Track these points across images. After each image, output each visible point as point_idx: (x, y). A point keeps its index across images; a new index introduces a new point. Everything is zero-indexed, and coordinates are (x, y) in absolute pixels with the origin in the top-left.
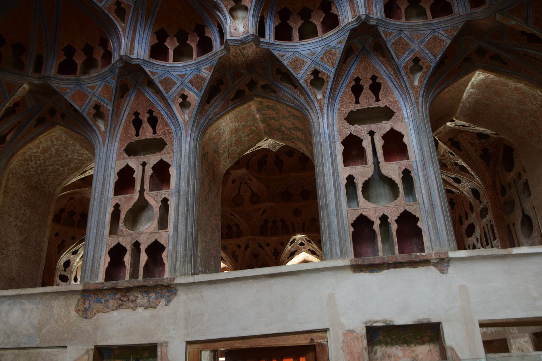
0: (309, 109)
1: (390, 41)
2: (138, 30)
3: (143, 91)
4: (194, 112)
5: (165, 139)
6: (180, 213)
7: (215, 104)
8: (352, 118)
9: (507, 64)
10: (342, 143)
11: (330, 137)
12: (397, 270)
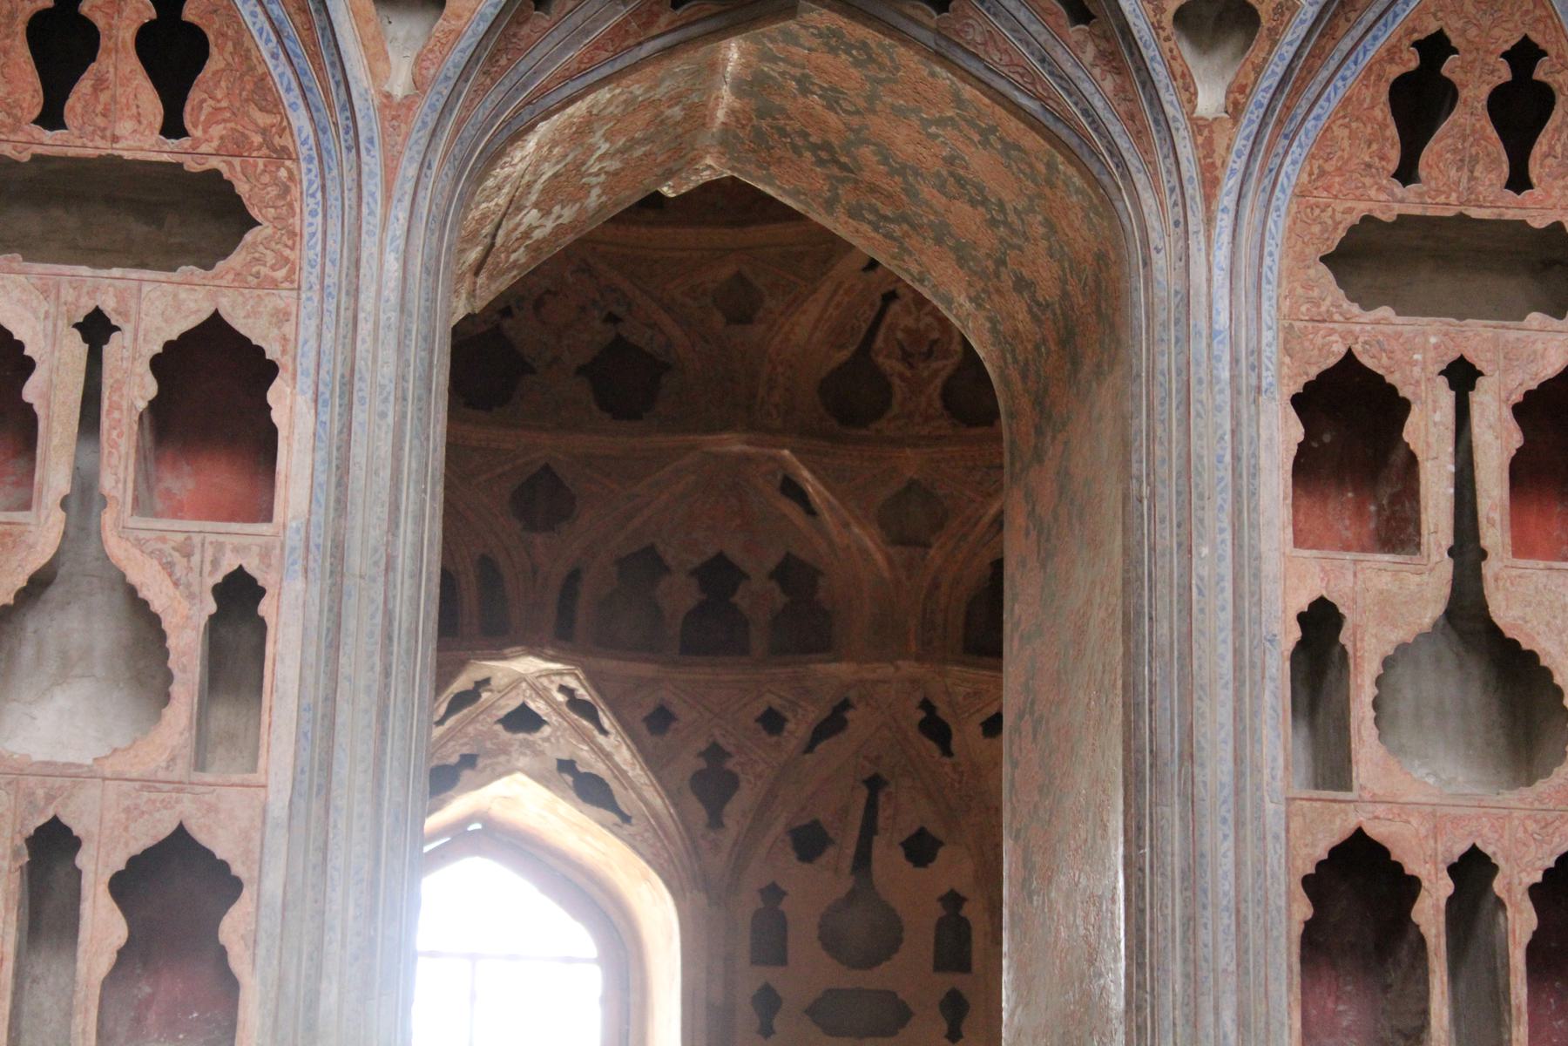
0: (1133, 162)
4: (457, 57)
5: (242, 188)
6: (344, 686)
7: (578, 18)
8: (1367, 258)
10: (1298, 402)
11: (1235, 361)
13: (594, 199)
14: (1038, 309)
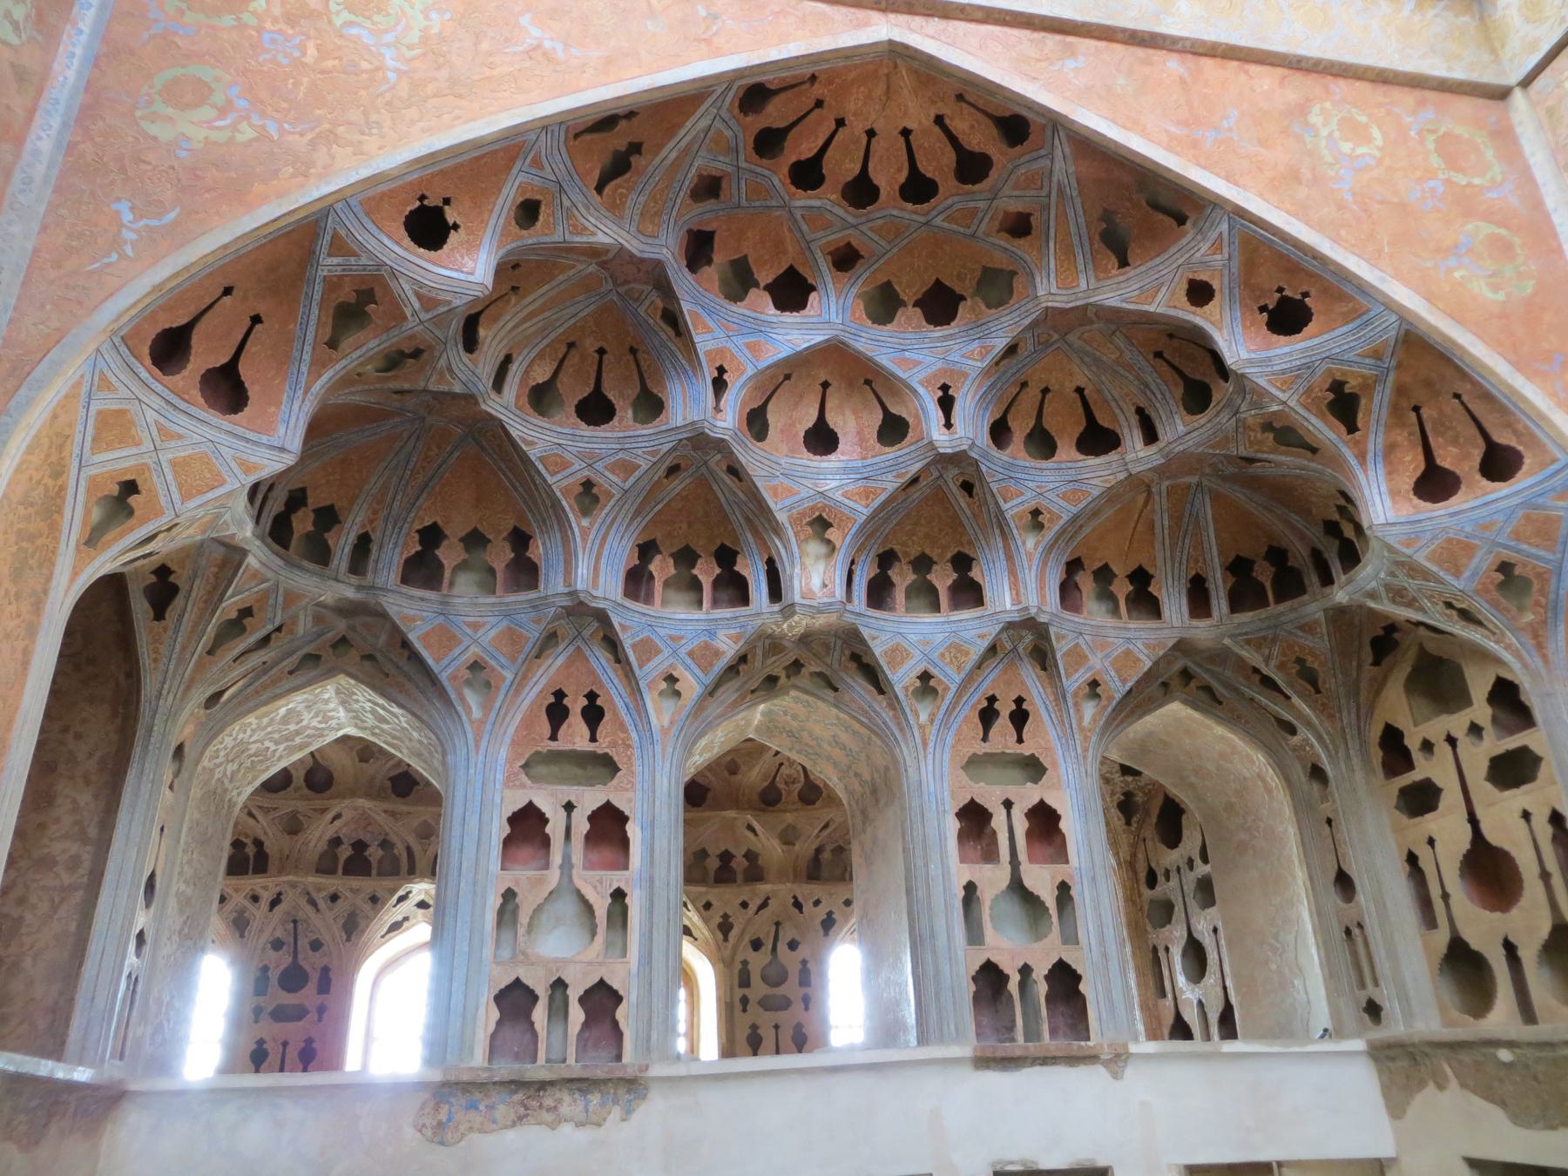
0: (899, 738)
1: (1061, 648)
2: (610, 538)
3: (588, 653)
4: (685, 713)
8: (974, 764)
9: (1220, 703)
12: (1045, 1069)
13: (716, 750)
14: (862, 783)
